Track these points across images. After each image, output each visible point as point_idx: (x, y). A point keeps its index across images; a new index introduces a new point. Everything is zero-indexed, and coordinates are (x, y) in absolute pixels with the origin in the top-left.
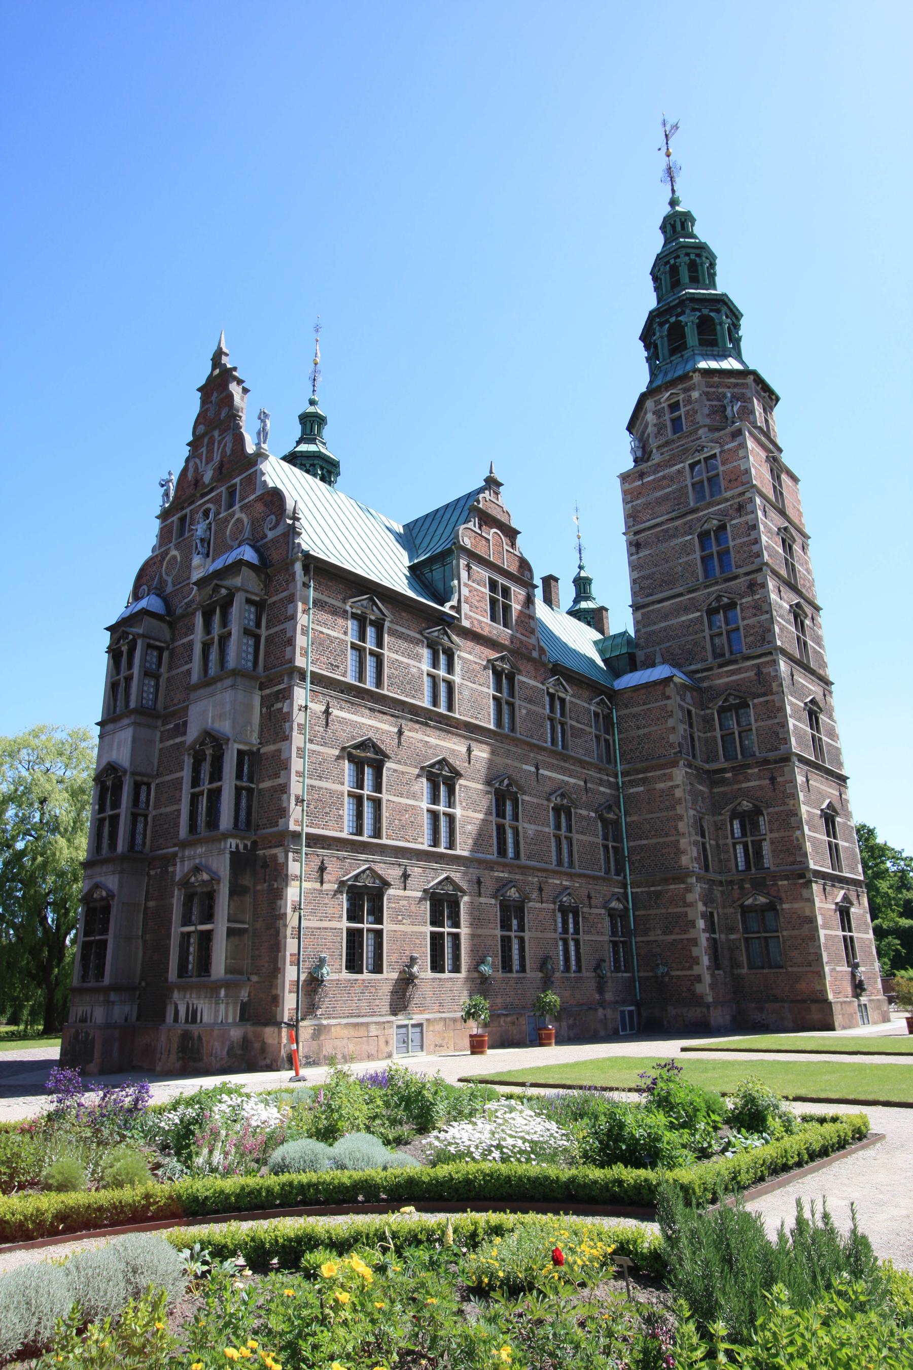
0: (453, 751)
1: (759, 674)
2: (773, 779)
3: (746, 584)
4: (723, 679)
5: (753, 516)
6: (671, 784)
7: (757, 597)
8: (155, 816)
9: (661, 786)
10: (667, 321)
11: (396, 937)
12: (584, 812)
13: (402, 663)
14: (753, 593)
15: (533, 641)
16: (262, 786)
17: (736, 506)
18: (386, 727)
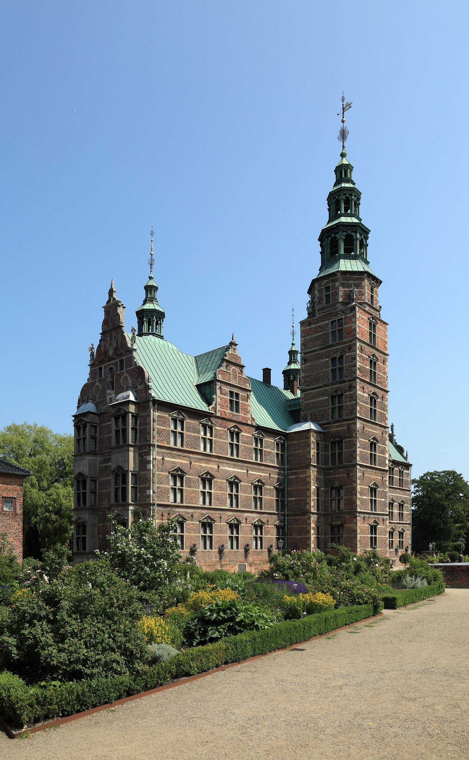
0: (211, 468)
1: (349, 428)
2: (348, 474)
3: (348, 385)
4: (334, 429)
5: (355, 353)
6: (306, 475)
7: (352, 392)
8: (99, 493)
9: (302, 476)
10: (330, 236)
11: (188, 538)
12: (268, 487)
13: (191, 435)
14: (351, 390)
15: (249, 416)
16: (140, 486)
17: (348, 347)
18: (185, 462)
